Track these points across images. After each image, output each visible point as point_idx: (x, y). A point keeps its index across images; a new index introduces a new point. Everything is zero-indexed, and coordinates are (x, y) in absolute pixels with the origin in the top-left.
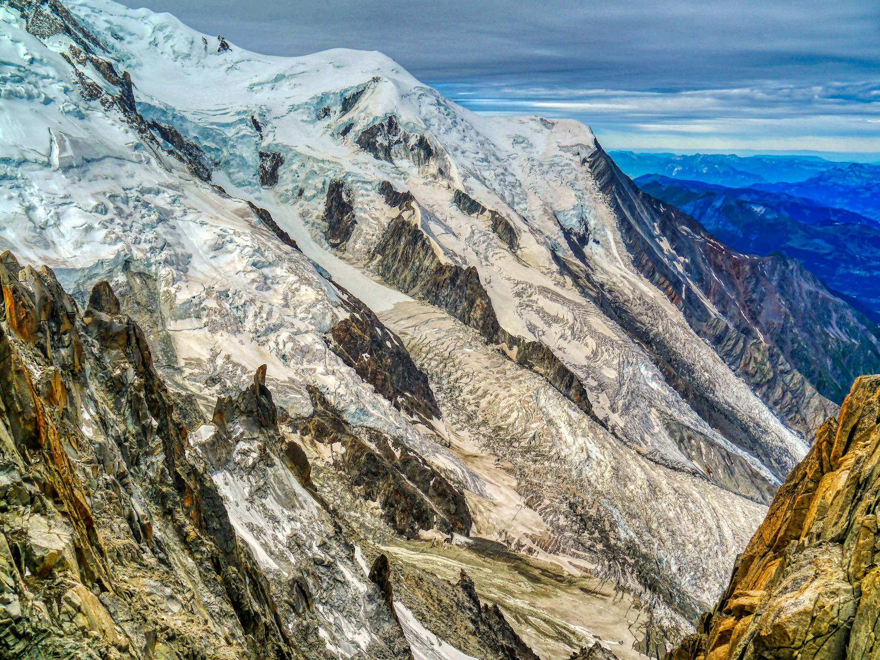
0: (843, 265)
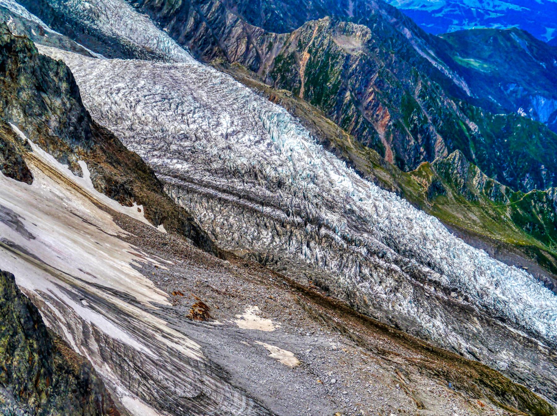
0: (456, 22)
